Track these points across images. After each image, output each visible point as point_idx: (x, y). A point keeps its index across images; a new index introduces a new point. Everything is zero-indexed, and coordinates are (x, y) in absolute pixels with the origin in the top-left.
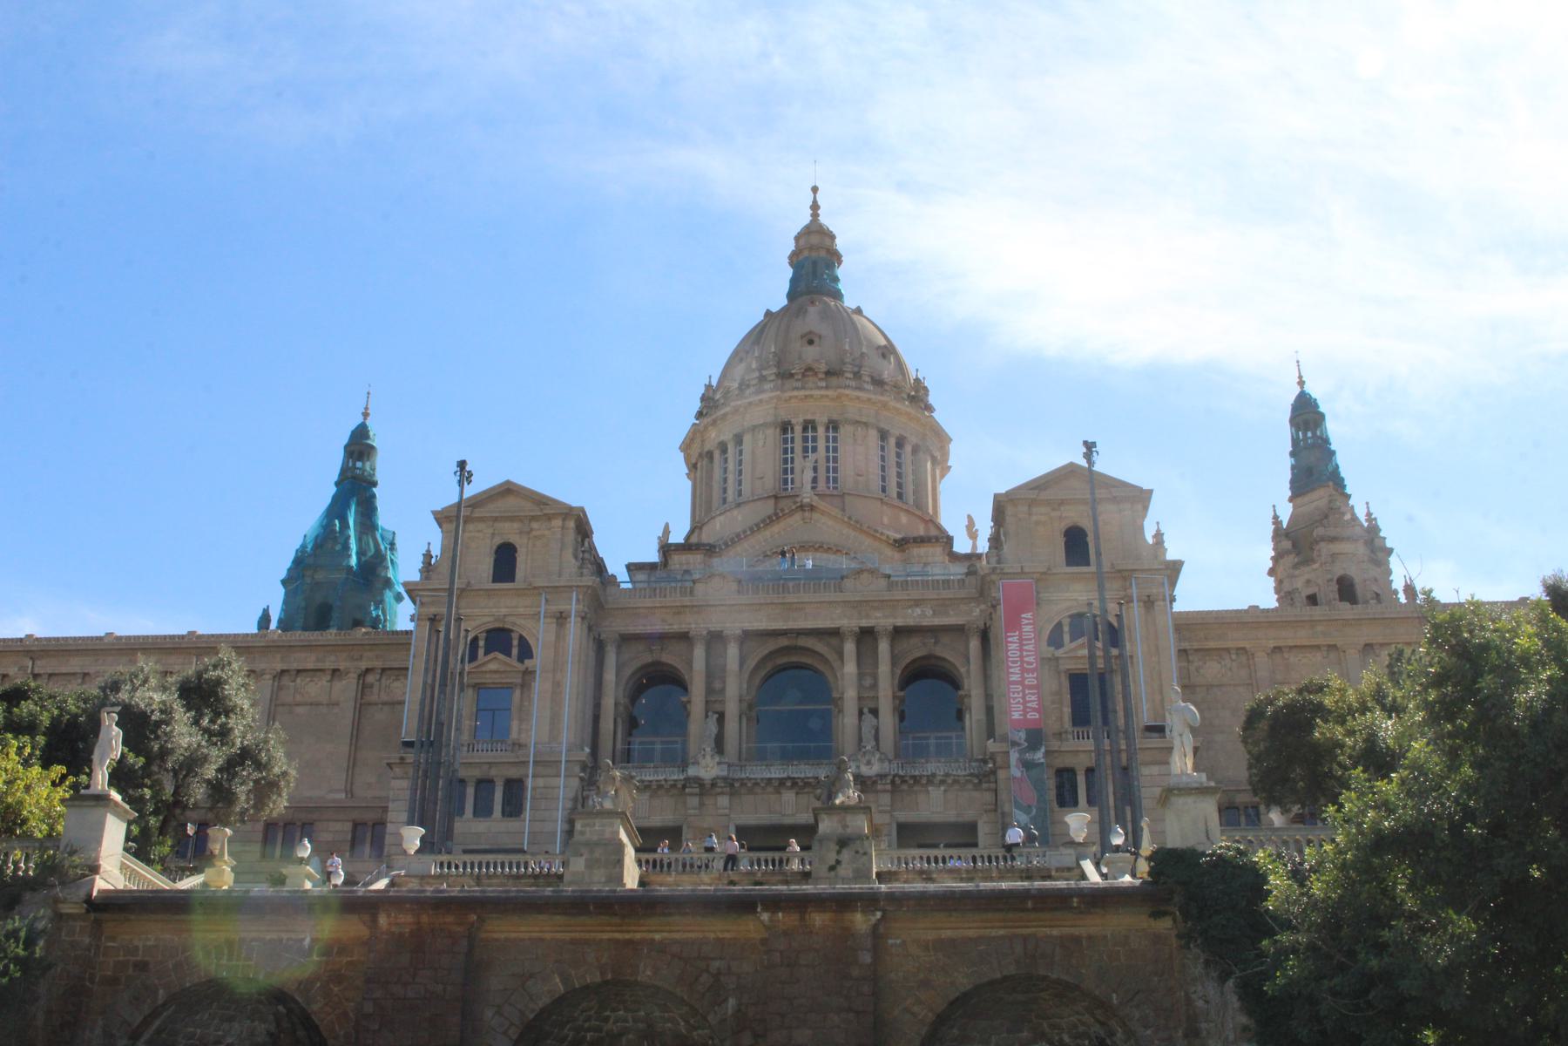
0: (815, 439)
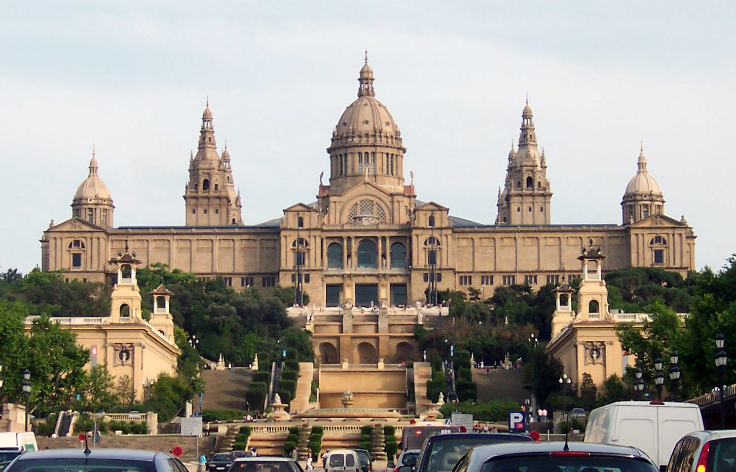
0: (368, 157)
